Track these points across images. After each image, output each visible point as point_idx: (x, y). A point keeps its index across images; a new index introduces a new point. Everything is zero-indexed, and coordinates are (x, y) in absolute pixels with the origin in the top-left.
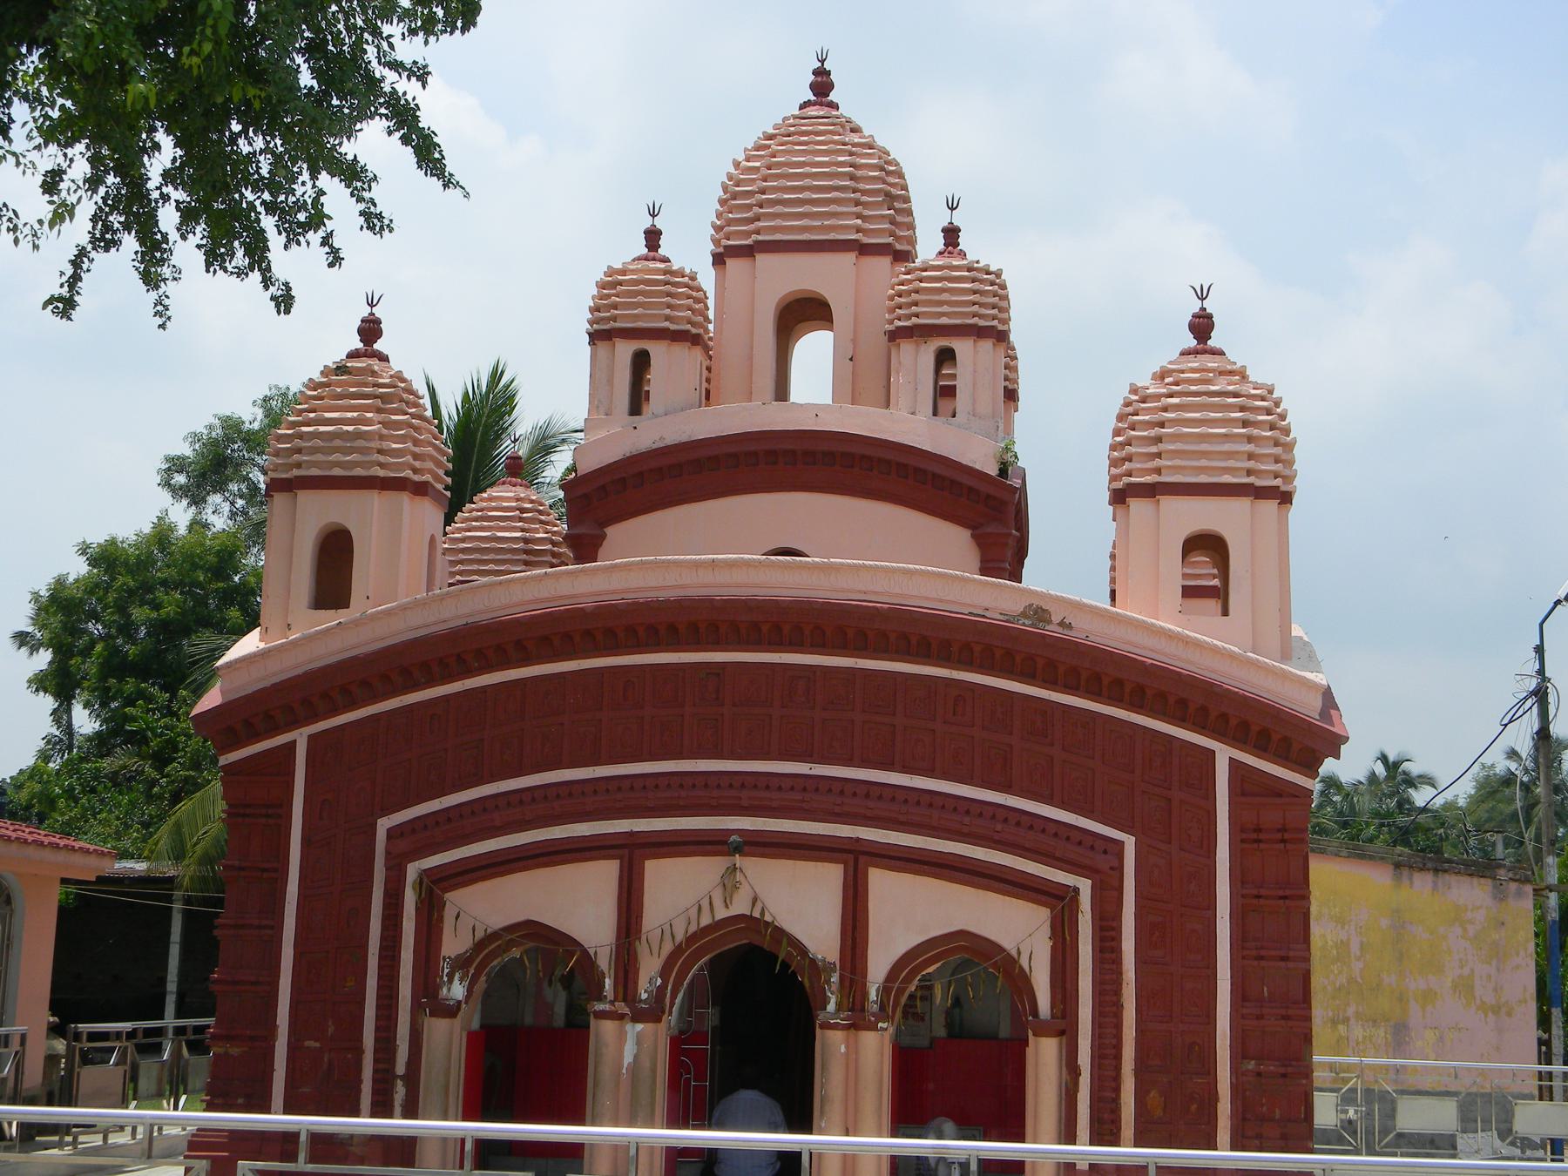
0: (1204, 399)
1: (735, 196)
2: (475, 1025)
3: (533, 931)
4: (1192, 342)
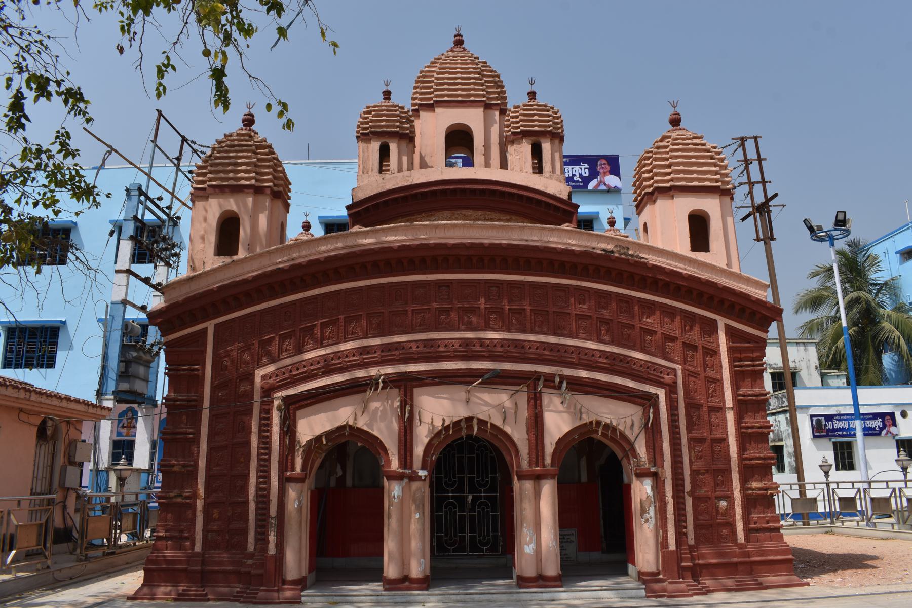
0: (691, 146)
2: (313, 488)
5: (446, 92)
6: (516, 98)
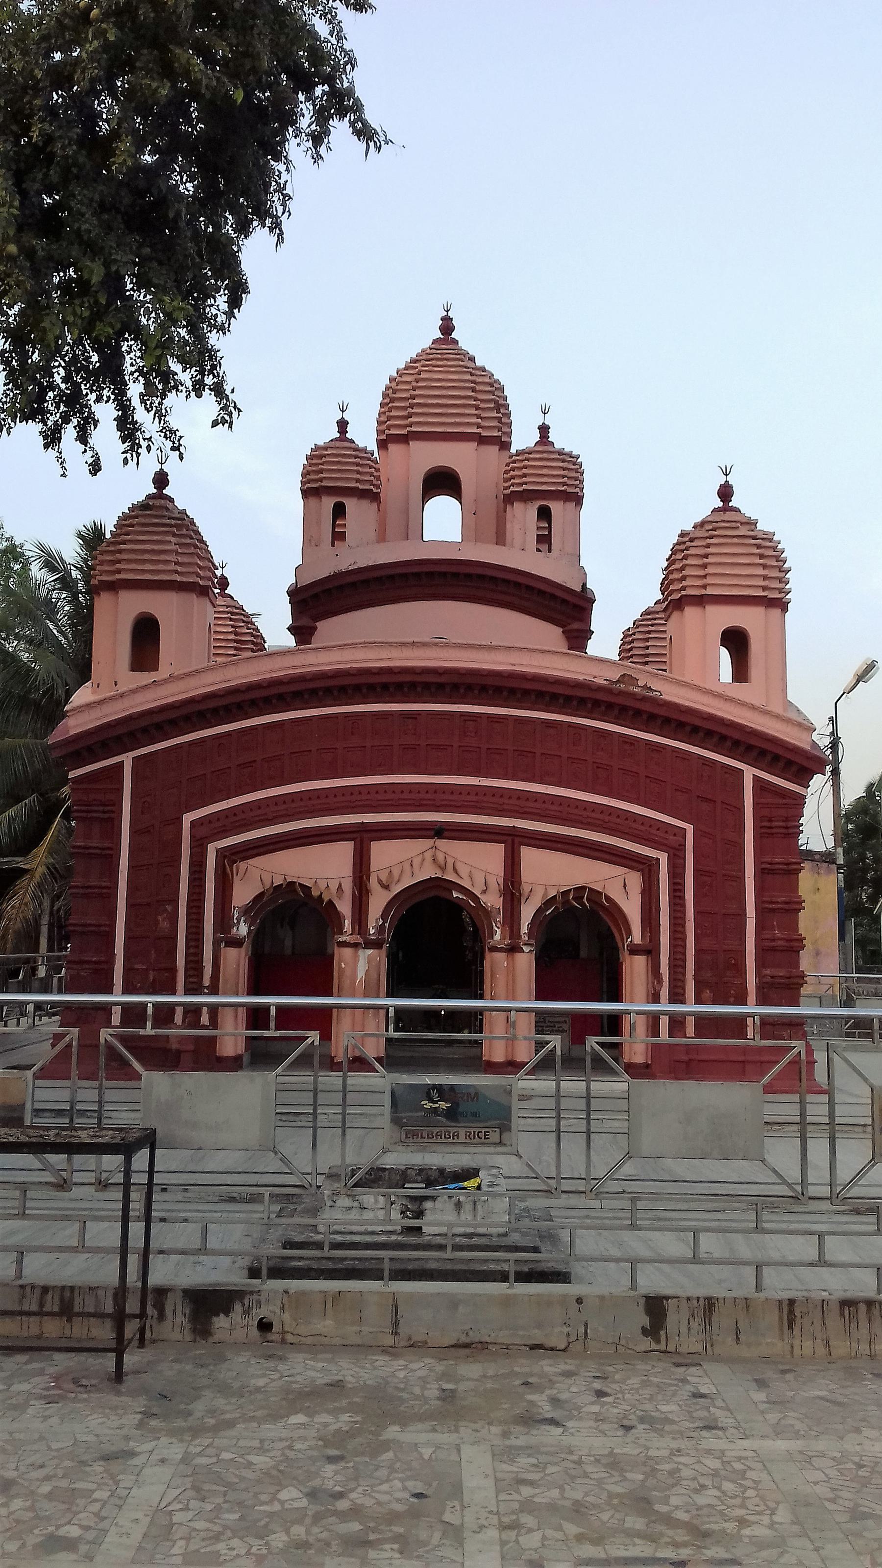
0: (735, 540)
1: (392, 400)
6: (523, 437)
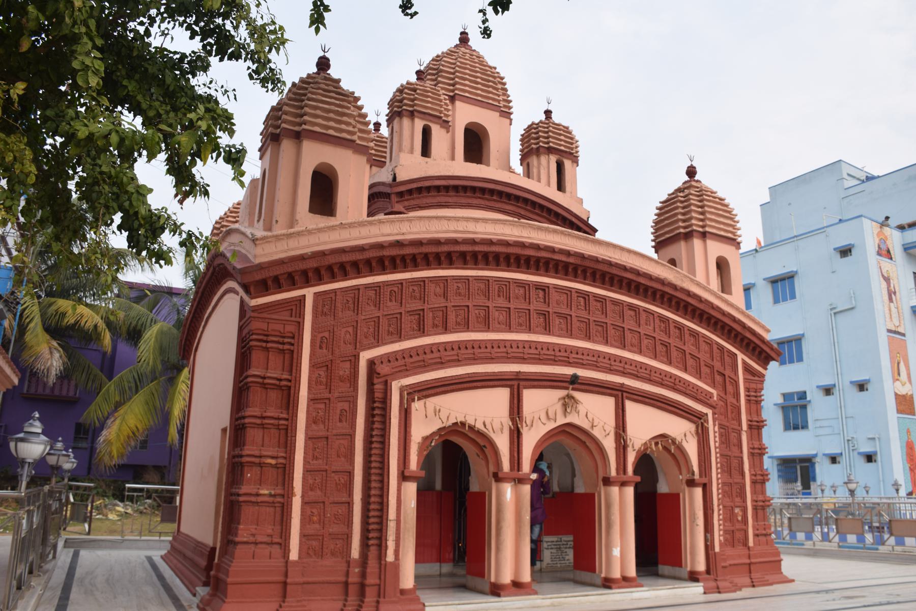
3: (459, 428)
4: (687, 178)
5: (467, 88)
